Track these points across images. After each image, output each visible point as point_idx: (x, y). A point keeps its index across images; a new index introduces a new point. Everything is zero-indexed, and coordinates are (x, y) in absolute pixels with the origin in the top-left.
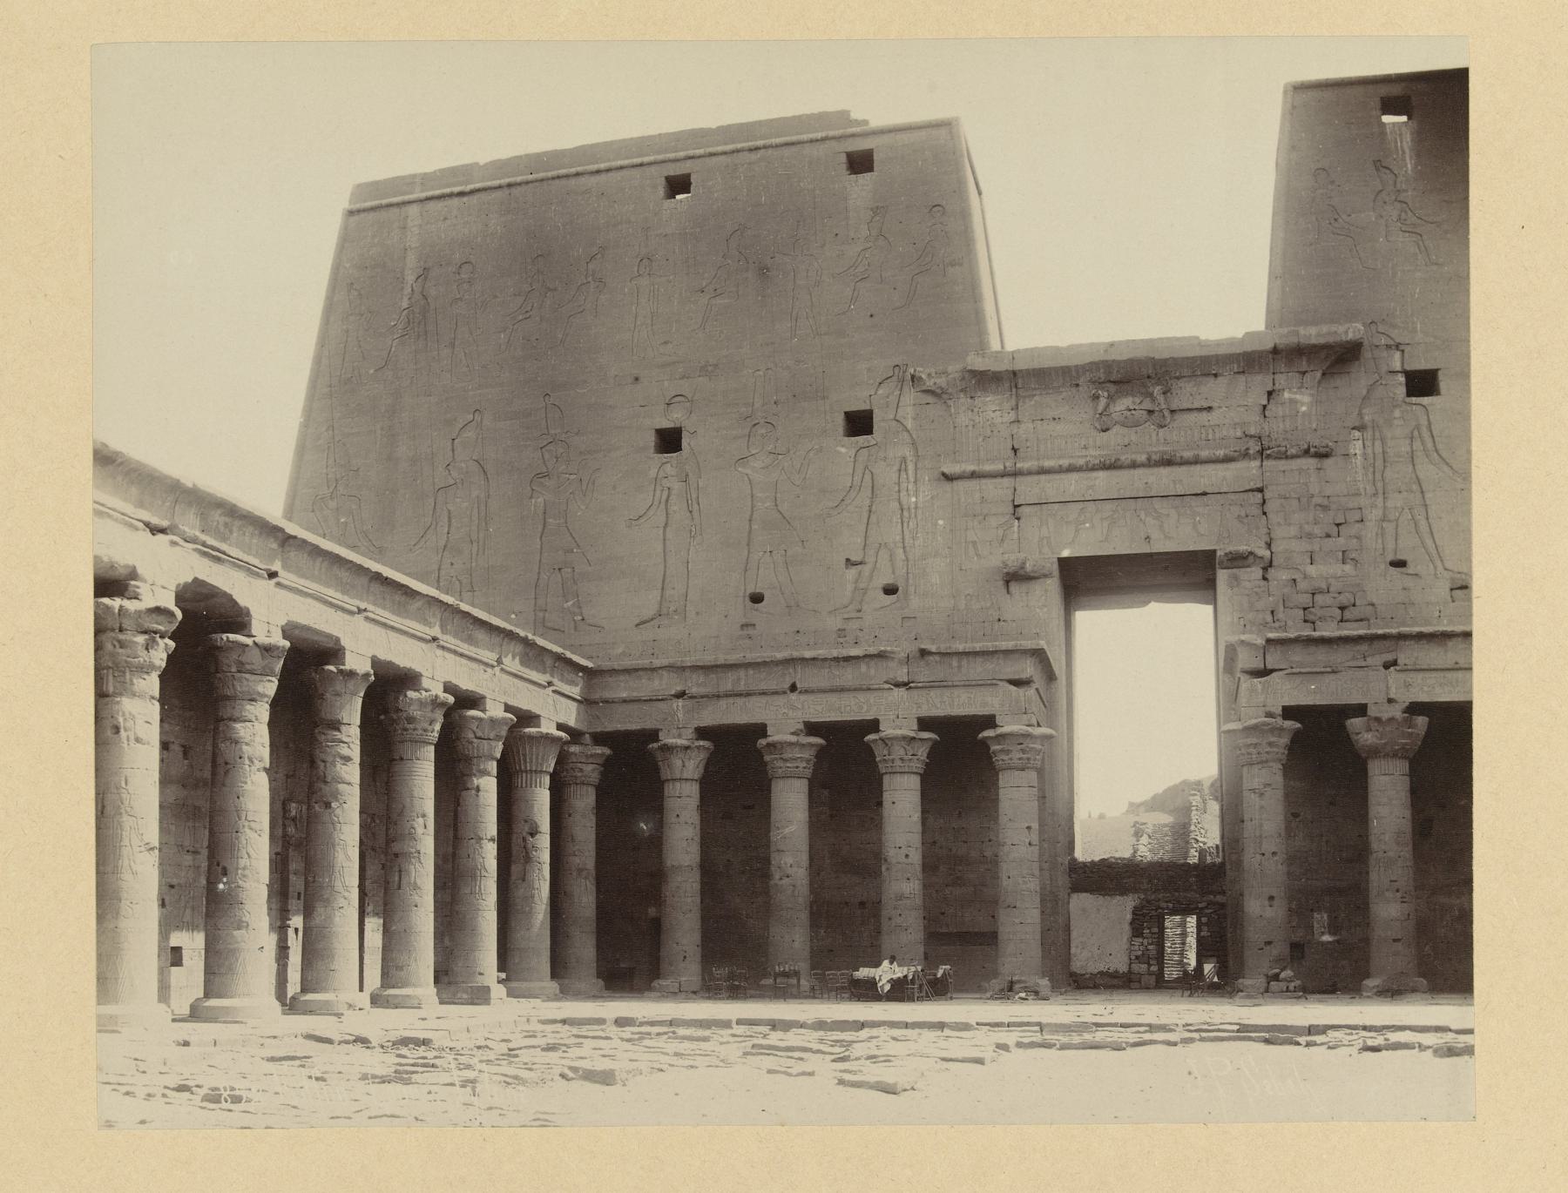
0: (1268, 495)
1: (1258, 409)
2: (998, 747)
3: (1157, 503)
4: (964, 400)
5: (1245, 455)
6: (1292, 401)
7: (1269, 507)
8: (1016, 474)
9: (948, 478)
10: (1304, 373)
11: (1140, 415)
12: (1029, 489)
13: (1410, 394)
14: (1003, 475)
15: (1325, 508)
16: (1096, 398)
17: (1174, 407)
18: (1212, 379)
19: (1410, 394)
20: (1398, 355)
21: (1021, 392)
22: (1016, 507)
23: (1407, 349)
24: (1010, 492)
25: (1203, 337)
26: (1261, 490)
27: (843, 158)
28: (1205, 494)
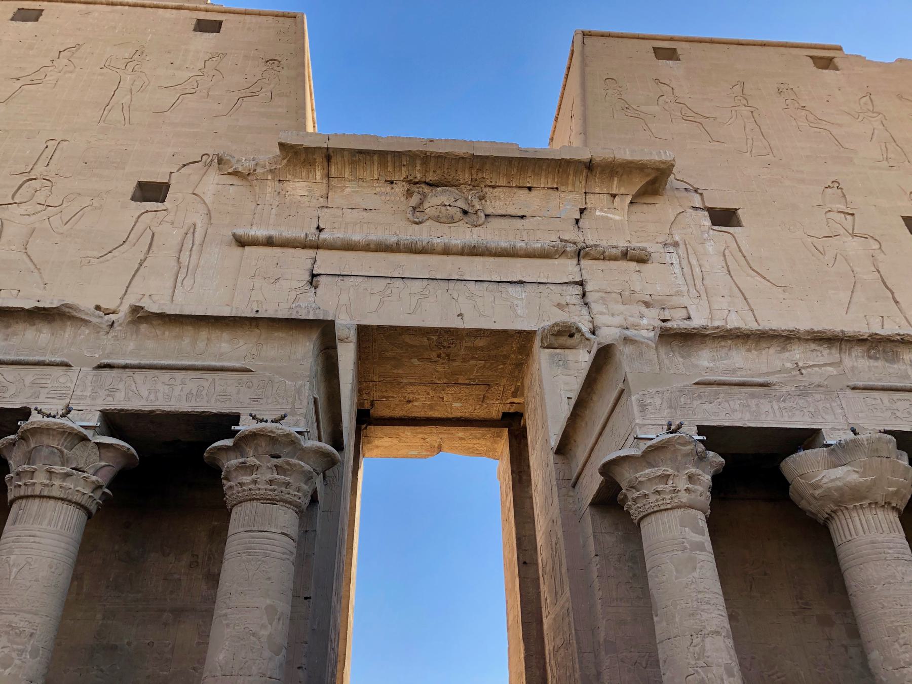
0: (588, 288)
1: (574, 222)
2: (234, 462)
3: (471, 285)
4: (271, 186)
5: (563, 253)
6: (602, 216)
7: (590, 298)
8: (316, 246)
9: (242, 243)
10: (614, 196)
11: (456, 212)
12: (327, 261)
13: (714, 224)
14: (305, 245)
15: (647, 305)
16: (409, 194)
17: (489, 211)
18: (527, 191)
19: (714, 224)
20: (698, 195)
21: (334, 182)
22: (314, 276)
23: (705, 193)
24: (310, 262)
25: (522, 146)
26: (581, 283)
27: (194, 22)
28: (521, 282)
